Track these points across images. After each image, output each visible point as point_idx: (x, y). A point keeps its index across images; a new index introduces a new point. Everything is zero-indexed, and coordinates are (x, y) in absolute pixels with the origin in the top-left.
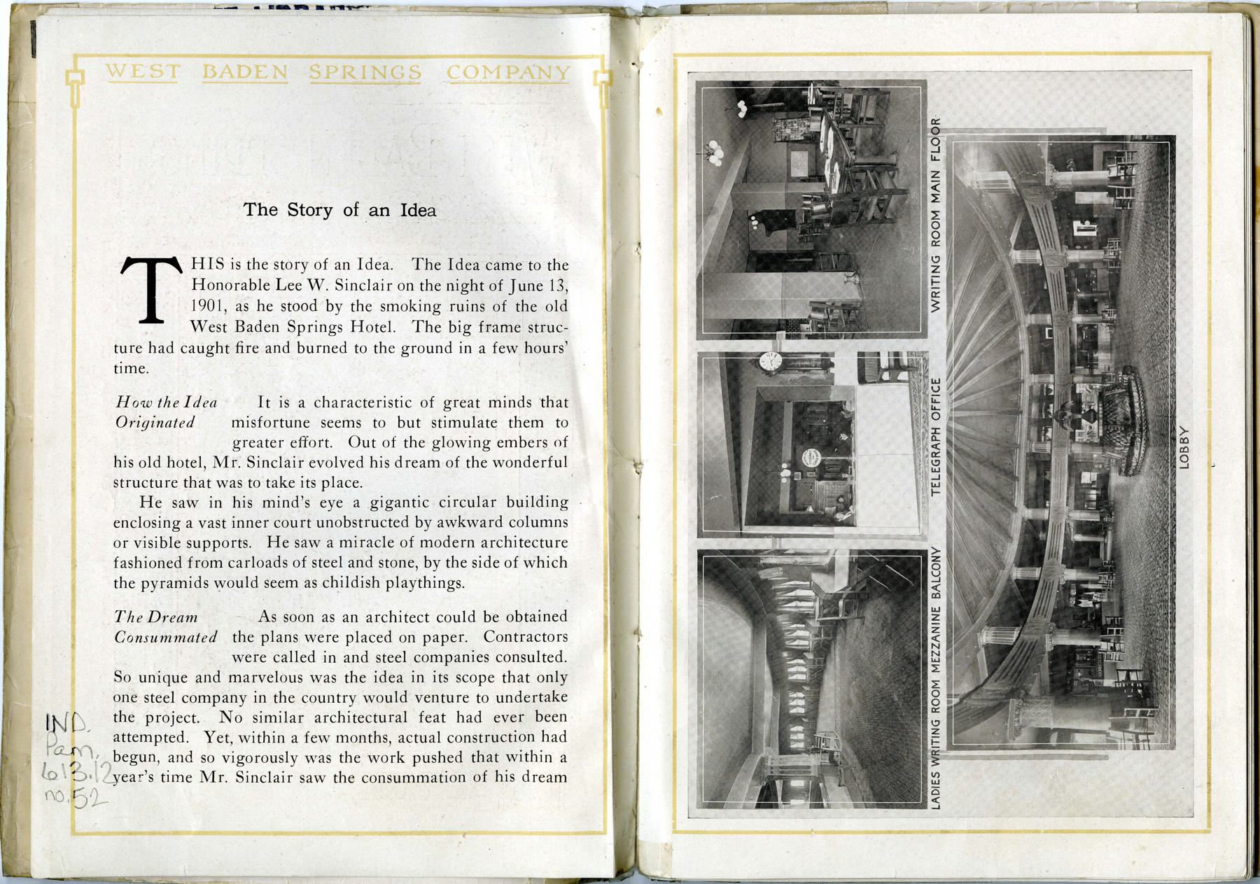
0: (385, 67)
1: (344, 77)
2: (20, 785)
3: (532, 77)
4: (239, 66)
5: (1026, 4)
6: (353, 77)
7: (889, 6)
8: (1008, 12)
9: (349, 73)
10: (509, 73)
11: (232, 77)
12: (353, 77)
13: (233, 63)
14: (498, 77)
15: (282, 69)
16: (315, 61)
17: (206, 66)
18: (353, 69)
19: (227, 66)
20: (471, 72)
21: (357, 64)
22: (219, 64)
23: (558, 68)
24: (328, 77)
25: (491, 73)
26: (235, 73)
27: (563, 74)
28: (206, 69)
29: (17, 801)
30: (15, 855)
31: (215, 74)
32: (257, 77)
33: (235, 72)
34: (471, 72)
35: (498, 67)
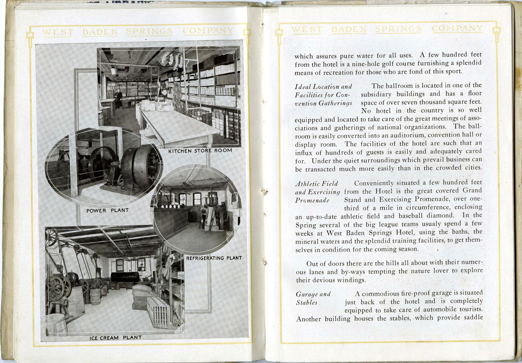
0: (157, 29)
1: (141, 33)
2: (9, 322)
3: (218, 32)
4: (98, 30)
5: (423, 1)
6: (144, 33)
7: (367, 2)
8: (416, 4)
9: (142, 32)
10: (208, 31)
11: (94, 34)
12: (144, 33)
13: (95, 29)
14: (204, 33)
15: (115, 31)
16: (129, 27)
17: (84, 30)
18: (144, 30)
19: (93, 30)
20: (193, 31)
21: (145, 27)
22: (89, 29)
23: (229, 28)
24: (134, 34)
25: (201, 31)
26: (96, 33)
27: (231, 31)
28: (84, 31)
29: (8, 329)
30: (7, 351)
31: (88, 33)
32: (105, 34)
33: (96, 32)
34: (193, 31)
35: (204, 29)
